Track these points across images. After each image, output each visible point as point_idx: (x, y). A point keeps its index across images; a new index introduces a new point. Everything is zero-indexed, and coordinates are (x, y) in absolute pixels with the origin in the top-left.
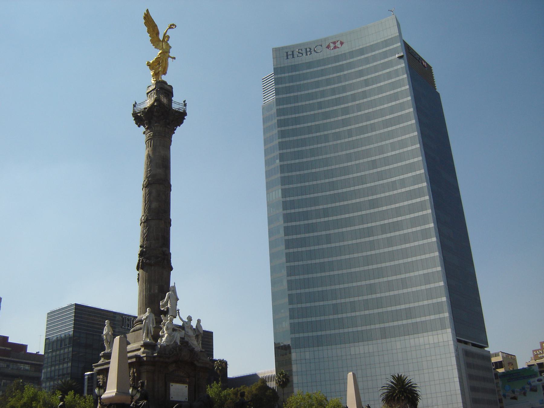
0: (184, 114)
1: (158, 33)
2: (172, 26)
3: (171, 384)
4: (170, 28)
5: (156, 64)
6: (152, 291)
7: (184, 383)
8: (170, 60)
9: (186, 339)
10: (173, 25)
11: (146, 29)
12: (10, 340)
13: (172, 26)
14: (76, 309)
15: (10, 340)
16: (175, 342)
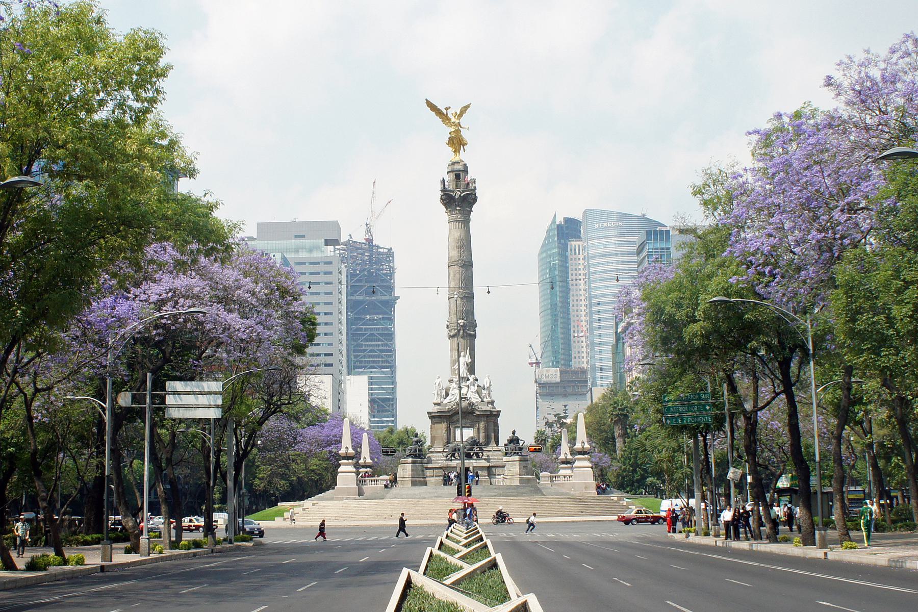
7: (468, 427)
13: (446, 109)
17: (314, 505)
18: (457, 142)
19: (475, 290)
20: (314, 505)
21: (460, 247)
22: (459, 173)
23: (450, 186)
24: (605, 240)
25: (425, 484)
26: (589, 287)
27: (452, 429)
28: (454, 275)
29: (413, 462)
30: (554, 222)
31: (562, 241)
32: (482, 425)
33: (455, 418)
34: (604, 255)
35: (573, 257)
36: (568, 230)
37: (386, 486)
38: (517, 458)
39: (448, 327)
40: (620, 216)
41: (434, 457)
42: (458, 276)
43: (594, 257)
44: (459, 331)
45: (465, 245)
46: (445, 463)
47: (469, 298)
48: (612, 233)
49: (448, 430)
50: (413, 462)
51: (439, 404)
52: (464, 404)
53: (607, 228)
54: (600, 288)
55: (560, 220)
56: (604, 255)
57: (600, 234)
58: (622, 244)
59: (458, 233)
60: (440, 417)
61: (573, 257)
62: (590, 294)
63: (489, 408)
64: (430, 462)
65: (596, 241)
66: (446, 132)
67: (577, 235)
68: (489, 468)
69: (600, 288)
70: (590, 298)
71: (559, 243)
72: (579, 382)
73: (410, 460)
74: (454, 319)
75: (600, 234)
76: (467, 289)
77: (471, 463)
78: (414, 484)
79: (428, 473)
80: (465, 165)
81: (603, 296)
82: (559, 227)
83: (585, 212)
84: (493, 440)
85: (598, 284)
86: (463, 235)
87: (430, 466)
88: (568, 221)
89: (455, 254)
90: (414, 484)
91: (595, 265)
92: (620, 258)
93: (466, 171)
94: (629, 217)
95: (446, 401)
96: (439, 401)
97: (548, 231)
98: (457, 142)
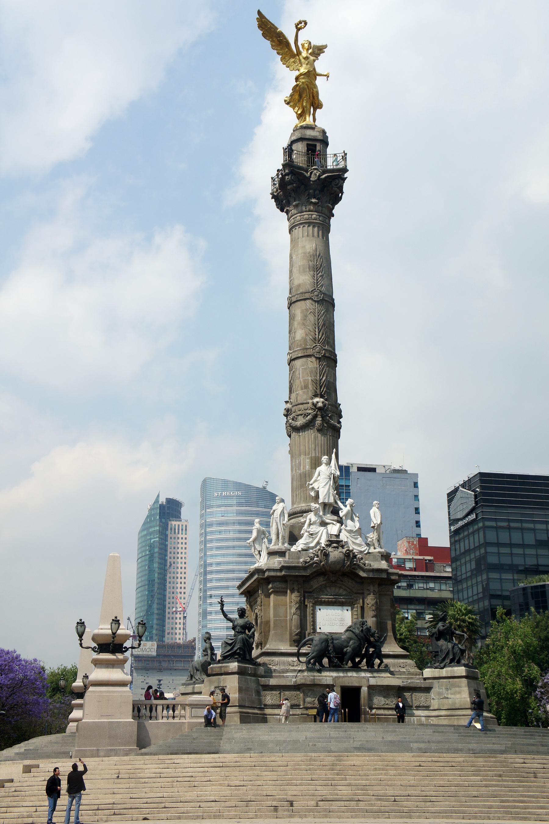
0: (345, 170)
1: (288, 44)
2: (300, 26)
3: (317, 607)
4: (298, 29)
5: (297, 97)
6: (302, 467)
7: (341, 604)
8: (320, 82)
9: (343, 537)
10: (300, 22)
11: (268, 43)
12: (431, 544)
14: (482, 481)
15: (430, 544)
16: (318, 543)
17: (27, 769)
18: (305, 97)
19: (337, 352)
20: (27, 769)
21: (316, 269)
22: (314, 144)
23: (299, 159)
24: (223, 509)
25: (263, 719)
26: (205, 554)
27: (309, 605)
28: (305, 317)
29: (241, 672)
30: (157, 501)
31: (163, 520)
32: (370, 600)
33: (316, 584)
34: (221, 524)
35: (173, 536)
36: (169, 510)
37: (209, 722)
38: (461, 670)
39: (288, 413)
40: (238, 486)
41: (276, 663)
42: (311, 318)
43: (211, 525)
44: (315, 416)
45: (321, 265)
46: (307, 677)
47: (329, 360)
48: (230, 502)
49: (302, 608)
50: (241, 672)
51: (282, 554)
52: (335, 554)
53: (226, 497)
54: (216, 556)
55: (162, 500)
56: (221, 524)
57: (219, 502)
58: (239, 513)
59: (309, 244)
60: (283, 579)
61: (173, 536)
62: (205, 561)
63: (383, 565)
64: (269, 673)
65: (214, 509)
66: (287, 78)
67: (177, 516)
68: (400, 691)
69: (216, 556)
70: (205, 565)
71: (161, 521)
72: (174, 656)
73: (234, 666)
74: (302, 395)
75: (219, 502)
76: (328, 343)
77: (362, 678)
78: (245, 719)
79: (269, 698)
80: (324, 132)
81: (219, 564)
82: (162, 507)
83: (205, 481)
84: (390, 634)
85: (214, 552)
86: (320, 248)
87: (273, 682)
88: (169, 501)
89: (305, 280)
90: (245, 719)
91: (212, 532)
92: (238, 527)
93: (325, 142)
94: (248, 488)
95: (294, 549)
96: (280, 546)
97: (151, 510)
98: (305, 97)
